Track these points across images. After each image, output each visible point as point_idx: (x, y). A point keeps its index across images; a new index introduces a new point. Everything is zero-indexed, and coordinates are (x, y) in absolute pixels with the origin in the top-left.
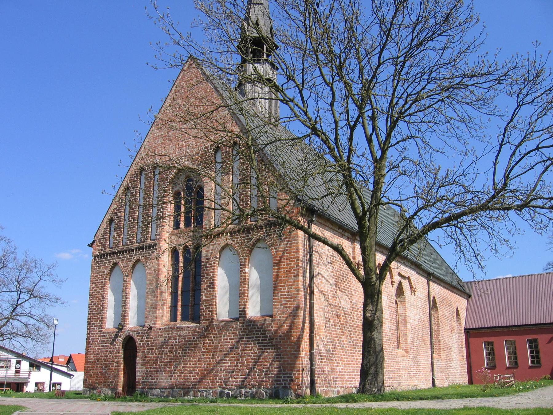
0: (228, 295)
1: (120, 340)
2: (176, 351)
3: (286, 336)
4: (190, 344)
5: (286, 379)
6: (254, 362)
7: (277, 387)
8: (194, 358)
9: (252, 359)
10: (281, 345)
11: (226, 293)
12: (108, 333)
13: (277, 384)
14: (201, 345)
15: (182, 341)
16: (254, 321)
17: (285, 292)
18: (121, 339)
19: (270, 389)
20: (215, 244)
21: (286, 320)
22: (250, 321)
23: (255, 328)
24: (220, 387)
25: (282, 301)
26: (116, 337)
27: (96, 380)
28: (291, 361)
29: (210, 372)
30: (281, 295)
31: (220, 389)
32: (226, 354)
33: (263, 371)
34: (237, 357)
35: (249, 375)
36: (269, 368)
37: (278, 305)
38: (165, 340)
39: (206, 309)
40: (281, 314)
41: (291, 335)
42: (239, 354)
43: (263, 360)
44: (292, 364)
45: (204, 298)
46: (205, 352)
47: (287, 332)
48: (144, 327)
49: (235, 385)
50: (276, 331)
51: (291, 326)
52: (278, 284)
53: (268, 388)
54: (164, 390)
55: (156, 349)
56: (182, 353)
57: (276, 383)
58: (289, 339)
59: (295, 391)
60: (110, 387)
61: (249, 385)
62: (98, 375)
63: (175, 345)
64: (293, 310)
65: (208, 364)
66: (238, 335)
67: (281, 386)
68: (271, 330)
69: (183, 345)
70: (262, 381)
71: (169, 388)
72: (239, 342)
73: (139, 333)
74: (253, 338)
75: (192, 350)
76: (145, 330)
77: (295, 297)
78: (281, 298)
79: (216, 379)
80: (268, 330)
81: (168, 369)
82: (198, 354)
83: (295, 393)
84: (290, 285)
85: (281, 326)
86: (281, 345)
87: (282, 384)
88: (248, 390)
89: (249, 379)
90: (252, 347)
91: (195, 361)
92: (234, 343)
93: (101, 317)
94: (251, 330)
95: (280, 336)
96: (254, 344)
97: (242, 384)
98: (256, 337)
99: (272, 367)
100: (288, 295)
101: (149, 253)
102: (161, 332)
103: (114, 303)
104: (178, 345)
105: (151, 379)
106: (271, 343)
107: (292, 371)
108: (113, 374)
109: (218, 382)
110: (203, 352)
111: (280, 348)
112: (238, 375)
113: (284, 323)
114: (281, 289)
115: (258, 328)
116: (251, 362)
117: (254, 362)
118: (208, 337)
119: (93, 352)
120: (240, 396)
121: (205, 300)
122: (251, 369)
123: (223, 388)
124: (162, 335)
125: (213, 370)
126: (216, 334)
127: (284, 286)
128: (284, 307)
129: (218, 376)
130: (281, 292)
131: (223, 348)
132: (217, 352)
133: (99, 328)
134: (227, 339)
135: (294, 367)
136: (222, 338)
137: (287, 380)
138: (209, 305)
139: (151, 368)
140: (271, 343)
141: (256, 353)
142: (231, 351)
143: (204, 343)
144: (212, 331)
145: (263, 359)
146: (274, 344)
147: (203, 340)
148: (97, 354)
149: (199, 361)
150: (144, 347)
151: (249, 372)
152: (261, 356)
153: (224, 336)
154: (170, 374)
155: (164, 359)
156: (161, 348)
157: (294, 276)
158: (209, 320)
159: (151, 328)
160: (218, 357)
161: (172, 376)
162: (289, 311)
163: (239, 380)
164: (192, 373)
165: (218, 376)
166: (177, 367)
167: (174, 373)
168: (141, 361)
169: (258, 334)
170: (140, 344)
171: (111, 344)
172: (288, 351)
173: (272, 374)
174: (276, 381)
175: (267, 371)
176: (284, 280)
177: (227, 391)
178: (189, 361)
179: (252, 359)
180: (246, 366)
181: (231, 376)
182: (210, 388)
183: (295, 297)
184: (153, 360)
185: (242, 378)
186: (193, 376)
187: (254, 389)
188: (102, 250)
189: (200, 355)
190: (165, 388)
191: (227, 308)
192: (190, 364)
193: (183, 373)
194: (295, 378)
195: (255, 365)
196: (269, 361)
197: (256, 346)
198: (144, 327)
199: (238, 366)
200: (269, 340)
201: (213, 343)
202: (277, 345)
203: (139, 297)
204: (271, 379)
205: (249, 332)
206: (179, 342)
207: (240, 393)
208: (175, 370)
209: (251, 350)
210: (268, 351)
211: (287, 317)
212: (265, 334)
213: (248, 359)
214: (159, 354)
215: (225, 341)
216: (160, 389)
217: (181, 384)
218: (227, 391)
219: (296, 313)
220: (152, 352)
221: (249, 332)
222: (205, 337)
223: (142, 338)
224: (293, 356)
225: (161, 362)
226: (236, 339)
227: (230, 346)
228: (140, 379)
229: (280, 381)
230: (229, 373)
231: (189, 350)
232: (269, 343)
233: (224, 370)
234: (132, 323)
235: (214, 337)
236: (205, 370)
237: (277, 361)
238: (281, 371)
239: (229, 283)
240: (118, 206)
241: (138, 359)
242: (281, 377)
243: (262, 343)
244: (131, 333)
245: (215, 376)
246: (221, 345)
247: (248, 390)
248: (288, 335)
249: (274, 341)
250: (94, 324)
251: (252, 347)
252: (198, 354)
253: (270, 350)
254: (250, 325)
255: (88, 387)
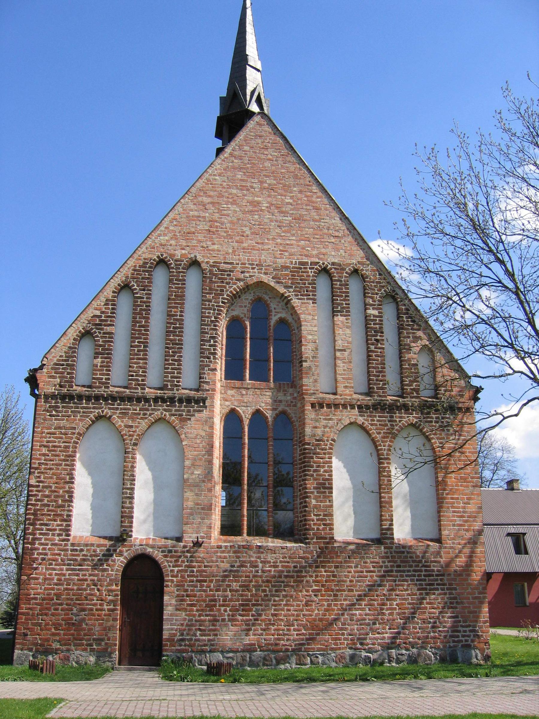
0: (351, 503)
1: (119, 562)
2: (257, 587)
3: (464, 571)
4: (286, 577)
5: (468, 633)
6: (413, 608)
7: (454, 646)
8: (297, 599)
9: (409, 604)
10: (457, 584)
11: (347, 500)
12: (87, 545)
13: (454, 641)
14: (311, 580)
15: (270, 571)
16: (404, 547)
17: (459, 508)
18: (122, 559)
19: (441, 650)
20: (330, 419)
21: (463, 547)
22: (400, 546)
23: (411, 557)
24: (351, 648)
25: (455, 521)
26: (108, 555)
27: (53, 634)
28: (474, 607)
29: (331, 624)
30: (454, 512)
31: (351, 652)
32: (359, 595)
33: (430, 623)
34: (382, 600)
35: (403, 628)
36: (438, 618)
37: (449, 525)
38: (233, 566)
39: (318, 520)
40: (453, 539)
41: (472, 571)
42: (384, 595)
43: (428, 606)
44: (476, 612)
45: (314, 502)
46: (318, 591)
47: (467, 566)
48: (179, 539)
49: (379, 644)
50: (448, 564)
51: (470, 557)
52: (447, 494)
53: (438, 648)
54: (231, 655)
55: (211, 581)
56: (270, 591)
57: (451, 640)
58: (469, 575)
59: (482, 651)
60: (92, 650)
61: (405, 643)
62: (60, 625)
63: (254, 576)
64: (474, 535)
65: (326, 610)
66: (381, 567)
67: (460, 645)
68: (439, 562)
69: (274, 577)
70: (427, 637)
71: (243, 651)
72: (384, 576)
73: (170, 551)
74: (408, 571)
75: (292, 586)
76: (185, 547)
77: (475, 517)
78: (453, 516)
79: (343, 634)
80: (435, 562)
81: (240, 618)
82: (305, 593)
83: (482, 654)
84: (468, 499)
85: (457, 557)
86: (457, 584)
87: (462, 641)
88: (404, 652)
89: (404, 634)
90: (408, 585)
91: (298, 605)
92: (375, 578)
93: (65, 513)
94: (402, 562)
95: (455, 571)
96: (412, 580)
97: (392, 643)
98: (415, 571)
99: (443, 617)
100: (464, 512)
101: (189, 411)
102: (223, 552)
103: (91, 491)
104: (261, 577)
105: (201, 635)
106: (441, 580)
107: (477, 621)
108: (101, 625)
109: (345, 639)
110: (313, 591)
111: (455, 589)
112: (384, 628)
113: (460, 552)
114: (453, 503)
115: (417, 557)
116: (408, 608)
117: (413, 608)
118: (323, 567)
119: (45, 579)
120: (390, 661)
121: (315, 506)
122: (408, 619)
123: (356, 649)
124: (225, 557)
125: (335, 620)
126: (341, 563)
127: (458, 498)
128: (459, 530)
129: (346, 629)
130: (453, 507)
131: (355, 586)
132: (344, 590)
133: (59, 535)
134: (362, 572)
135: (478, 617)
136: (352, 570)
137: (469, 636)
138: (325, 515)
139: (200, 615)
140: (441, 580)
141: (416, 594)
142: (369, 590)
143: (317, 576)
144: (332, 557)
145: (427, 603)
146: (446, 582)
147: (315, 571)
148: (56, 584)
149: (307, 605)
150: (182, 577)
151: (405, 623)
152: (424, 599)
153: (356, 567)
154: (244, 627)
155: (231, 600)
156: (223, 581)
157: (473, 486)
158: (326, 538)
159: (197, 544)
160: (345, 600)
161: (249, 630)
162: (469, 535)
163: (386, 635)
164: (293, 625)
165: (346, 629)
166: (260, 615)
167: (254, 625)
168: (173, 602)
169: (418, 566)
170: (172, 571)
171: (95, 567)
172: (469, 593)
173: (444, 627)
174: (451, 636)
175: (435, 622)
176: (457, 490)
177: (364, 654)
178: (285, 605)
179: (409, 604)
180: (399, 614)
181: (371, 629)
182: (332, 649)
183: (475, 517)
184: (204, 601)
185: (391, 633)
186: (294, 630)
187: (415, 650)
188: (61, 386)
189: (310, 596)
190: (235, 651)
191: (351, 522)
192: (289, 610)
193: (273, 625)
194: (482, 632)
195: (414, 613)
196: (438, 608)
197: (416, 585)
198: (179, 539)
199: (384, 614)
200: (437, 575)
201: (334, 576)
202: (450, 584)
203: (158, 486)
204: (443, 634)
205: (402, 562)
206: (263, 571)
207: (389, 656)
208: (256, 620)
209: (407, 590)
210: (436, 592)
211: (465, 544)
212: (429, 566)
213: (402, 604)
214: (217, 590)
215: (357, 575)
216: (222, 652)
217: (272, 644)
218: (364, 654)
219: (478, 539)
220: (202, 586)
221: (402, 562)
222: (317, 567)
223: (177, 561)
224: (477, 601)
225: (223, 605)
226: (379, 571)
227: (368, 583)
228: (175, 635)
229: (458, 636)
230: (368, 624)
231: (285, 586)
232: (437, 580)
233: (358, 620)
234: (143, 532)
235: (336, 567)
236: (321, 620)
237: (452, 608)
238: (460, 621)
239: (352, 483)
240: (103, 312)
241: (166, 598)
242: (459, 631)
243: (425, 580)
244: (149, 550)
245: (341, 629)
246: (351, 581)
247: (404, 652)
248: (467, 570)
249: (445, 578)
250: (46, 525)
251: (408, 585)
252: (305, 593)
253: (440, 591)
254: (403, 552)
255: (30, 650)
